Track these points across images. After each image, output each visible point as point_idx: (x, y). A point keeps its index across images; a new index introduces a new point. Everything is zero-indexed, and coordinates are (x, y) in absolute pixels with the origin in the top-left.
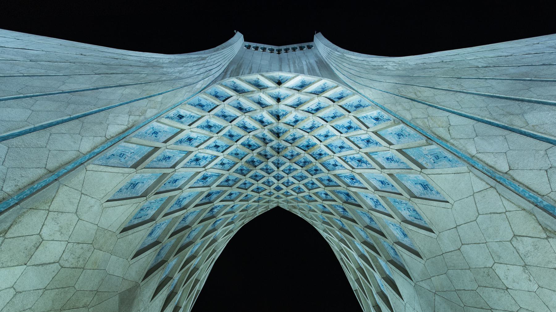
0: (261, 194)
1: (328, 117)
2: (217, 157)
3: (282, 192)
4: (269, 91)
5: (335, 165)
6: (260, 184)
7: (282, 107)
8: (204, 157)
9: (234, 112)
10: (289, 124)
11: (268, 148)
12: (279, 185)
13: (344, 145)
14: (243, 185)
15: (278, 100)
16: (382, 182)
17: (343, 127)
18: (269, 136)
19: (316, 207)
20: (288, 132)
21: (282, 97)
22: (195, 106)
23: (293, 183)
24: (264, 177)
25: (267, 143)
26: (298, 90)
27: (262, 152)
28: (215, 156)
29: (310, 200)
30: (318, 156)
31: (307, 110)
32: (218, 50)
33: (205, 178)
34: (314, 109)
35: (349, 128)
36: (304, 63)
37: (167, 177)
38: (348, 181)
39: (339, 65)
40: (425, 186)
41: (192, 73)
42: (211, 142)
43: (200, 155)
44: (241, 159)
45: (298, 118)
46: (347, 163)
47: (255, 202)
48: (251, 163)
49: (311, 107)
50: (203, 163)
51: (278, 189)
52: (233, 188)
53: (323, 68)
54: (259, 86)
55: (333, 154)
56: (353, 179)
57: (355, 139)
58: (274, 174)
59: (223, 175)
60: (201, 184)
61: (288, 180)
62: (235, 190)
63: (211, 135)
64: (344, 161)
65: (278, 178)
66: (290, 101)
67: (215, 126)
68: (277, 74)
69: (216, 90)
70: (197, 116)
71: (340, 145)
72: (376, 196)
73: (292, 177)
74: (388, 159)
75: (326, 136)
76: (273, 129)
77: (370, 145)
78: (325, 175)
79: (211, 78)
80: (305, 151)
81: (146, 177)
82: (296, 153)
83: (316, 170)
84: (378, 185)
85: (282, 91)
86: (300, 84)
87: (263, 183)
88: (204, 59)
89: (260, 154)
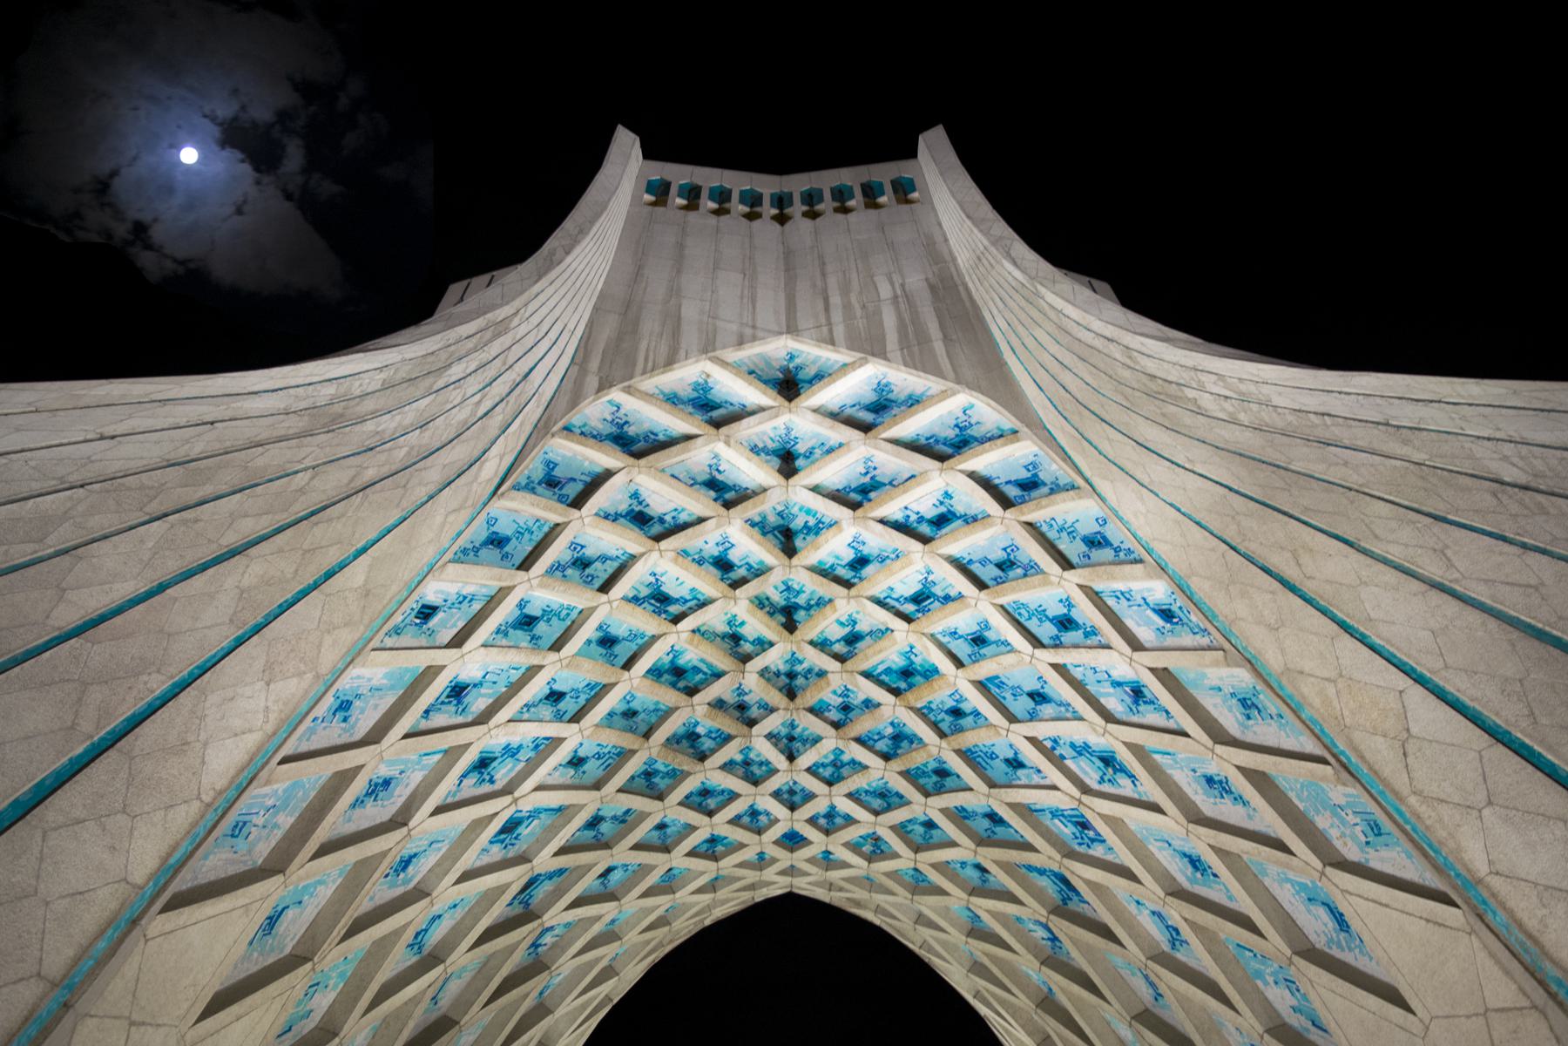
0: (723, 863)
1: (984, 562)
16: (1195, 862)
17: (1041, 613)
18: (756, 625)
21: (801, 448)
24: (733, 796)
30: (949, 719)
32: (551, 264)
33: (510, 827)
36: (885, 291)
39: (1020, 329)
42: (536, 688)
45: (866, 551)
47: (700, 891)
53: (955, 331)
57: (1090, 673)
58: (775, 783)
60: (497, 853)
61: (833, 807)
63: (535, 661)
65: (792, 799)
66: (837, 472)
67: (548, 614)
68: (777, 349)
69: (551, 456)
70: (484, 591)
71: (1032, 685)
73: (850, 796)
74: (1210, 780)
82: (862, 697)
84: (1181, 873)
86: (870, 397)
87: (735, 821)
88: (501, 328)
89: (719, 705)
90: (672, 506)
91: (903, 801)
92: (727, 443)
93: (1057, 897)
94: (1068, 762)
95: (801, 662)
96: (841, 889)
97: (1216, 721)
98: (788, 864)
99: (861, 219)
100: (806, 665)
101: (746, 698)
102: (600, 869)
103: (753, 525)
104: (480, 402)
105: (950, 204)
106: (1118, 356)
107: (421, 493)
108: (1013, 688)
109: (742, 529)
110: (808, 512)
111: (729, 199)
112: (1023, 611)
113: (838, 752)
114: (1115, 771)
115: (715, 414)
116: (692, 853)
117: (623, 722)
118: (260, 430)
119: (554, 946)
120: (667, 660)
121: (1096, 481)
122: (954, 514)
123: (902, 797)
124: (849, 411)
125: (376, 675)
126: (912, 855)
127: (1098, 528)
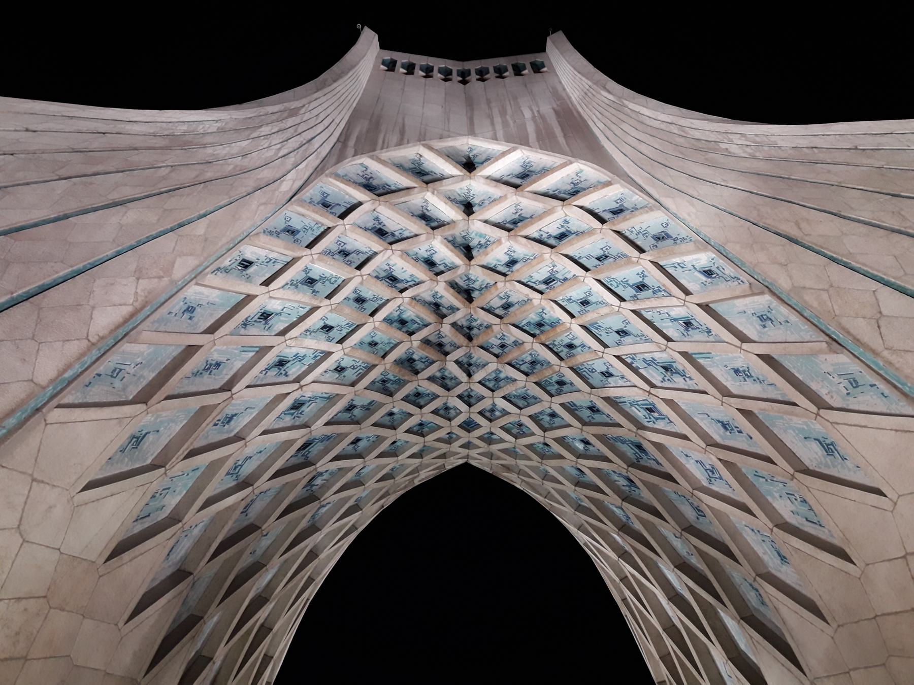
1: (588, 257)
2: (328, 354)
3: (478, 433)
4: (447, 187)
5: (608, 374)
6: (425, 415)
7: (477, 228)
8: (296, 355)
9: (366, 243)
10: (493, 270)
11: (446, 329)
12: (473, 416)
13: (628, 328)
14: (388, 418)
15: (468, 208)
16: (725, 426)
17: (625, 283)
18: (449, 298)
19: (561, 470)
20: (493, 290)
21: (476, 201)
22: (278, 234)
23: (505, 413)
24: (436, 397)
25: (443, 316)
26: (516, 186)
27: (432, 338)
28: (322, 352)
29: (544, 454)
31: (536, 235)
32: (324, 85)
33: (297, 406)
34: (554, 234)
35: (641, 287)
36: (527, 114)
37: (214, 415)
38: (640, 414)
39: (613, 127)
40: (829, 448)
41: (270, 153)
42: (314, 321)
43: (289, 353)
44: (384, 357)
45: (515, 256)
46: (636, 371)
47: (412, 456)
48: (406, 364)
49: (546, 229)
50: (294, 370)
51: (469, 426)
52: (363, 425)
53: (571, 131)
54: (423, 176)
55: (601, 348)
56: (650, 410)
58: (459, 390)
59: (339, 396)
60: (288, 421)
61: (494, 405)
62: (367, 431)
63: (316, 303)
64: (629, 366)
65: (468, 399)
66: (497, 213)
67: (324, 279)
69: (325, 189)
71: (619, 326)
72: (712, 458)
74: (737, 371)
75: (585, 303)
76: (458, 280)
77: (691, 332)
78: (582, 397)
79: (313, 162)
80: (533, 336)
81: (167, 419)
82: (513, 339)
83: (561, 383)
84: (717, 434)
85: (476, 186)
86: (518, 170)
87: (435, 412)
88: (294, 113)
89: (426, 342)
90: (399, 227)
91: (537, 400)
92: (433, 193)
93: (633, 457)
94: (641, 371)
95: (476, 320)
96: (498, 458)
97: (741, 332)
98: (466, 440)
99: (510, 79)
100: (479, 322)
101: (443, 340)
102: (351, 438)
103: (449, 241)
104: (280, 149)
105: (568, 71)
106: (676, 131)
107: (243, 190)
108: (606, 329)
109: (442, 242)
110: (481, 236)
111: (432, 71)
112: (613, 283)
113: (498, 371)
114: (672, 373)
115: (426, 178)
116: (408, 431)
117: (368, 348)
118: (138, 142)
119: (323, 486)
120: (396, 314)
121: (663, 200)
122: (570, 232)
123: (536, 398)
124: (505, 178)
125: (213, 293)
126: (542, 433)
127: (663, 229)
